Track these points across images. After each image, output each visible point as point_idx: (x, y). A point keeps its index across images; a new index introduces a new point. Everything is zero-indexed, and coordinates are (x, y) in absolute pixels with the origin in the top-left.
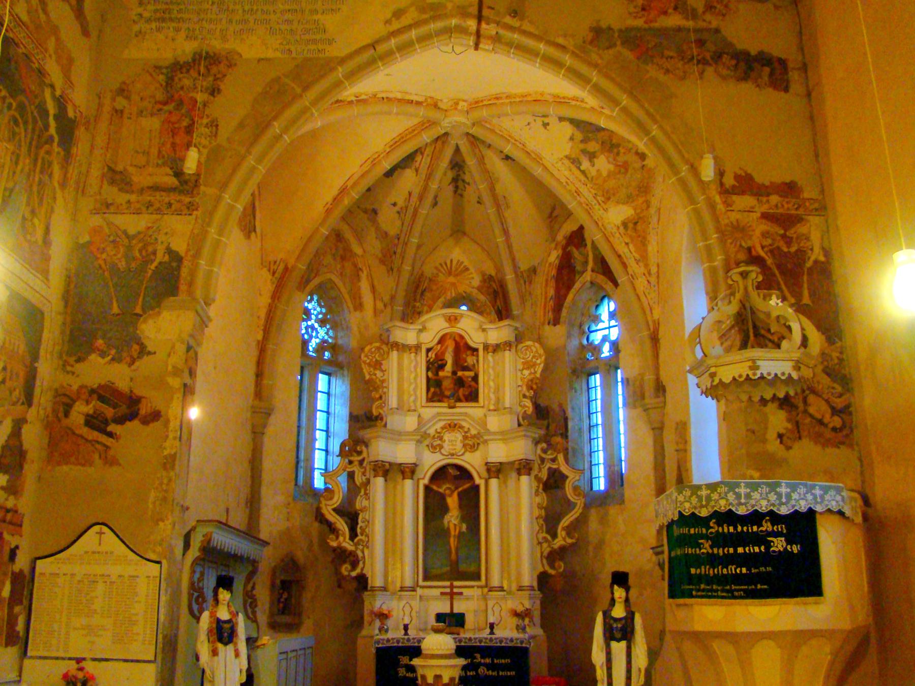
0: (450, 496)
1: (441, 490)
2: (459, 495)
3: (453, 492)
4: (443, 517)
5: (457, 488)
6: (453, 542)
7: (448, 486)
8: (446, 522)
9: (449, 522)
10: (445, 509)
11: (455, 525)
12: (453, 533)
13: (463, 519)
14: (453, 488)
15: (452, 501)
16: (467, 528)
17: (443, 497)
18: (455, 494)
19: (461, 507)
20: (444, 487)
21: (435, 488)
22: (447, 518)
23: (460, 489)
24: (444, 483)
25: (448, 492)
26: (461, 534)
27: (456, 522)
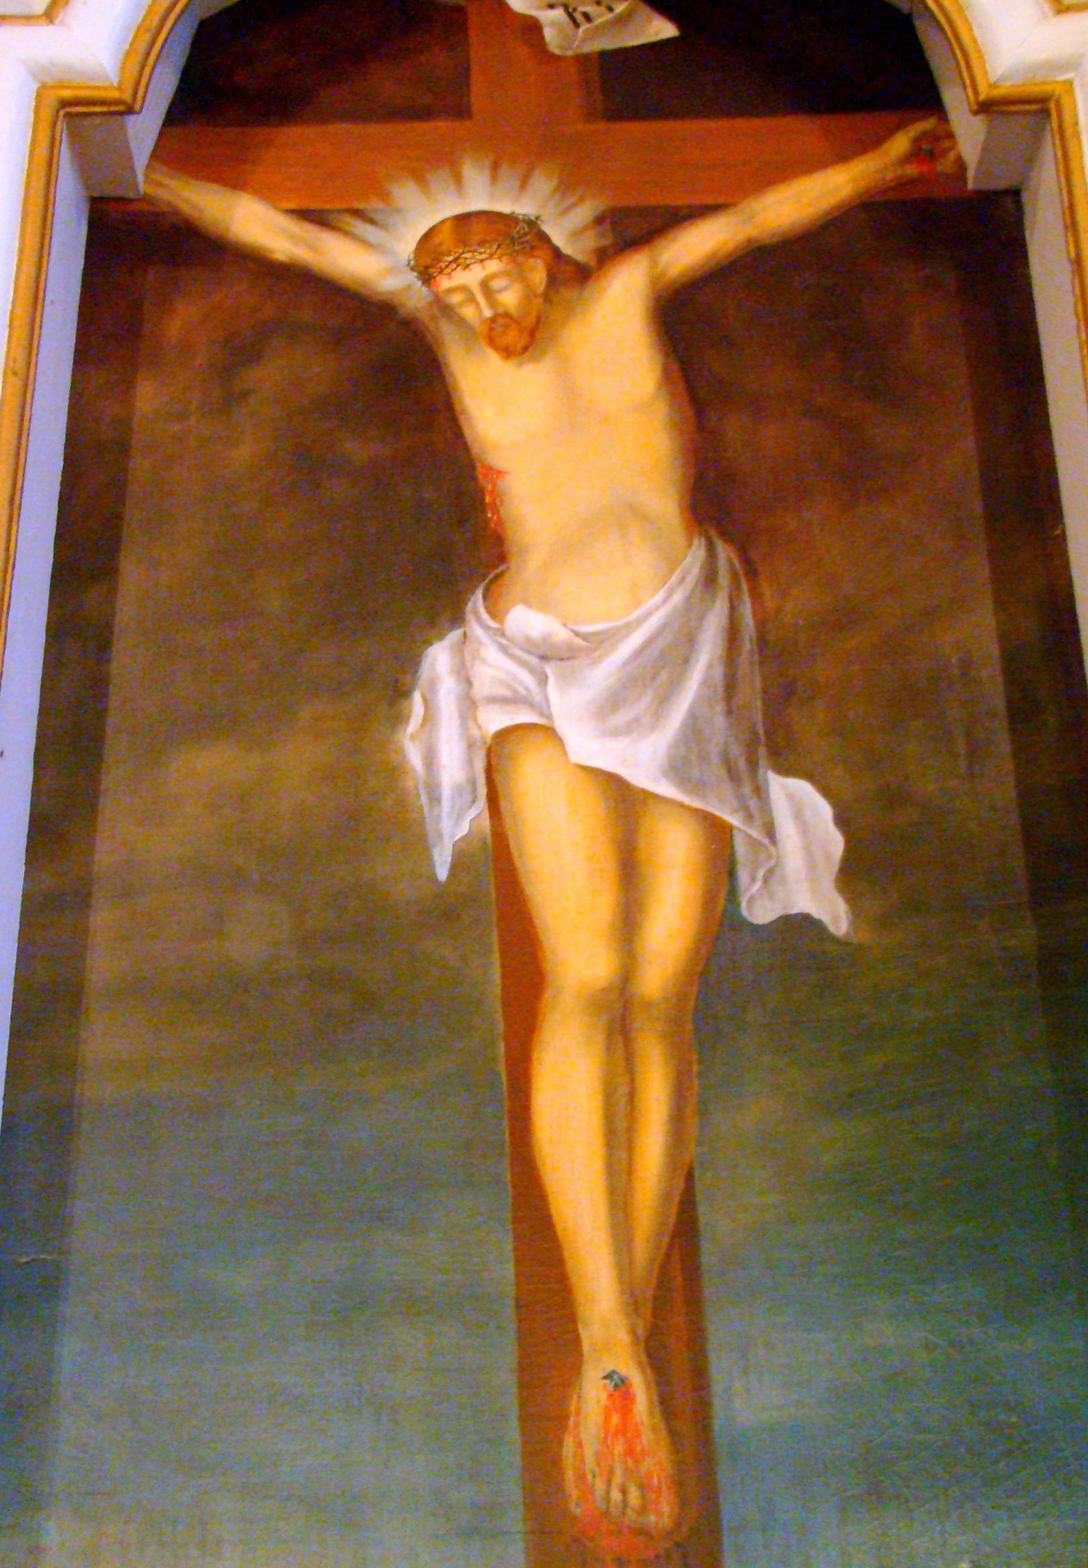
0: (524, 337)
1: (372, 260)
2: (683, 320)
3: (572, 276)
4: (396, 686)
5: (632, 229)
6: (585, 1126)
7: (480, 193)
8: (438, 741)
9: (496, 758)
10: (438, 538)
11: (623, 801)
12: (578, 952)
13: (777, 710)
14: (568, 230)
15: (572, 423)
16: (853, 874)
17: (391, 370)
18: (618, 312)
19: (717, 500)
20: (422, 210)
21: (254, 221)
22: (463, 688)
23: (694, 246)
24: (443, 161)
25: (479, 282)
26: (745, 986)
27: (643, 759)
